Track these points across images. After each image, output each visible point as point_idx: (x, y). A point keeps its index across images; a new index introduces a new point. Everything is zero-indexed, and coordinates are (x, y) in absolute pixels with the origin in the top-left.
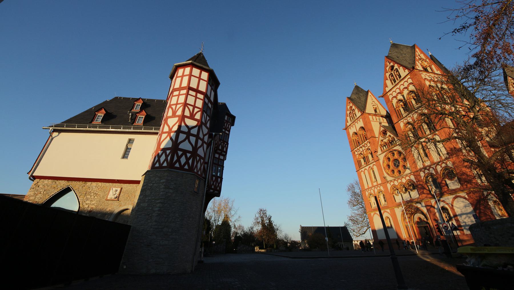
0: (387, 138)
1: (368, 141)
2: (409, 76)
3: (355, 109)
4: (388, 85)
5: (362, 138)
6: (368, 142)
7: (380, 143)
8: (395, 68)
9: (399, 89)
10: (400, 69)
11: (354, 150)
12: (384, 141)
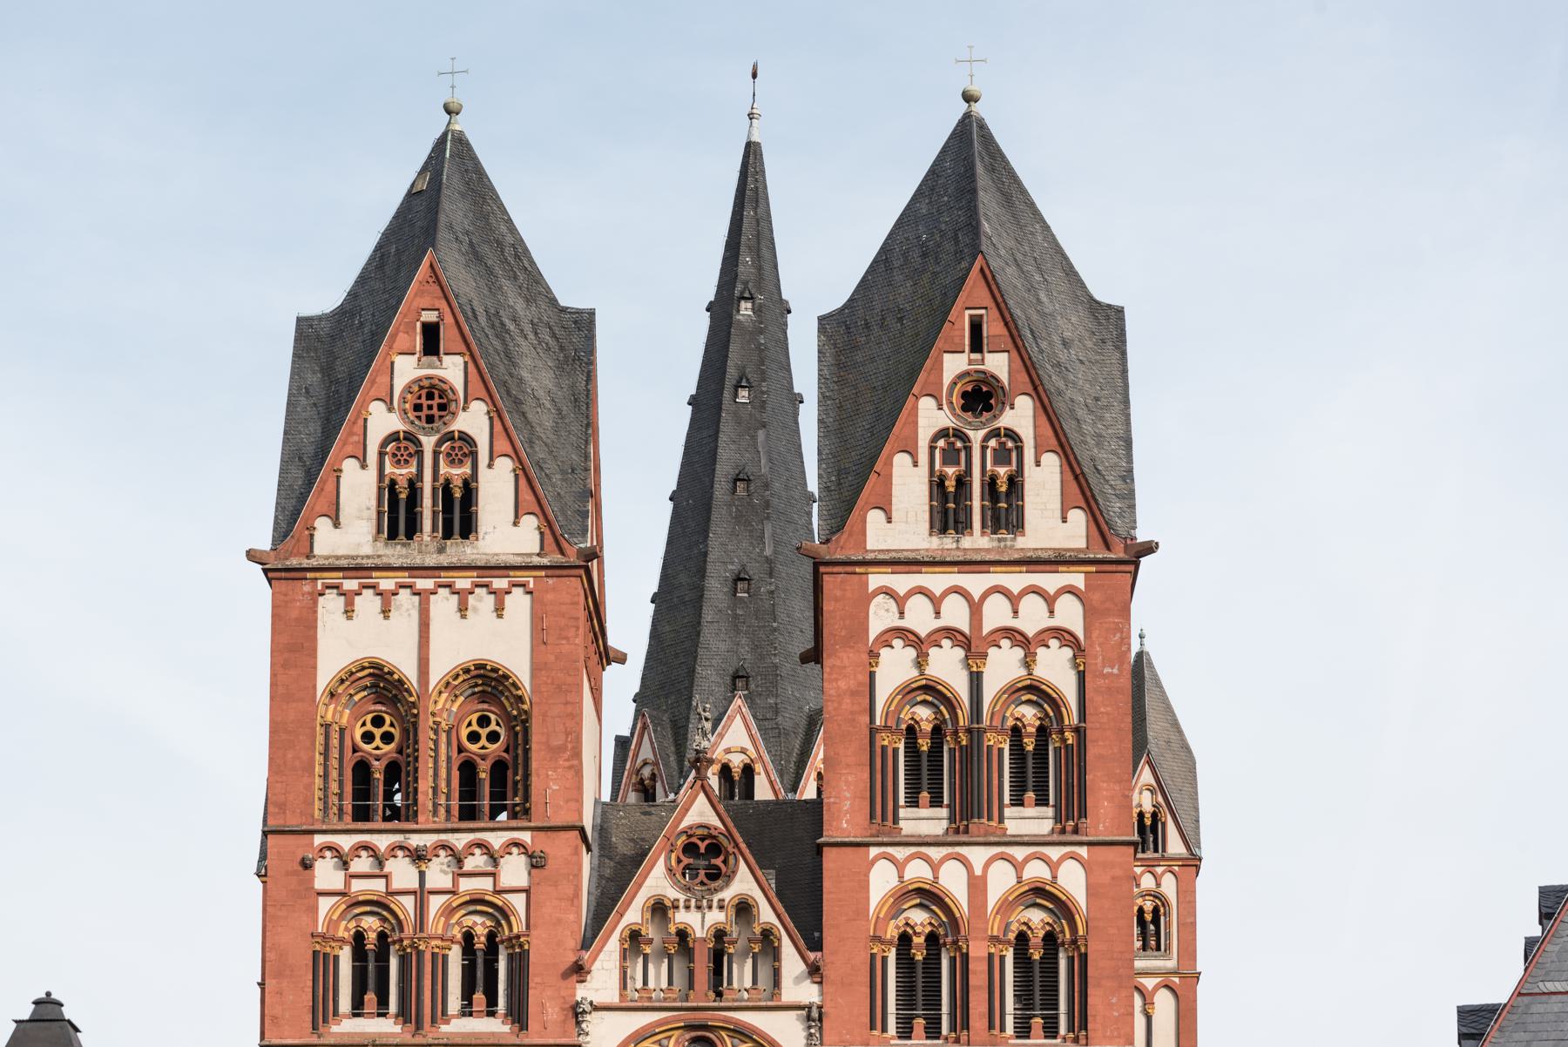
0: (721, 907)
1: (526, 837)
2: (1077, 579)
3: (490, 466)
4: (894, 500)
5: (443, 773)
6: (517, 844)
7: (633, 914)
8: (1007, 420)
9: (976, 609)
10: (1038, 464)
11: (319, 840)
12: (682, 917)
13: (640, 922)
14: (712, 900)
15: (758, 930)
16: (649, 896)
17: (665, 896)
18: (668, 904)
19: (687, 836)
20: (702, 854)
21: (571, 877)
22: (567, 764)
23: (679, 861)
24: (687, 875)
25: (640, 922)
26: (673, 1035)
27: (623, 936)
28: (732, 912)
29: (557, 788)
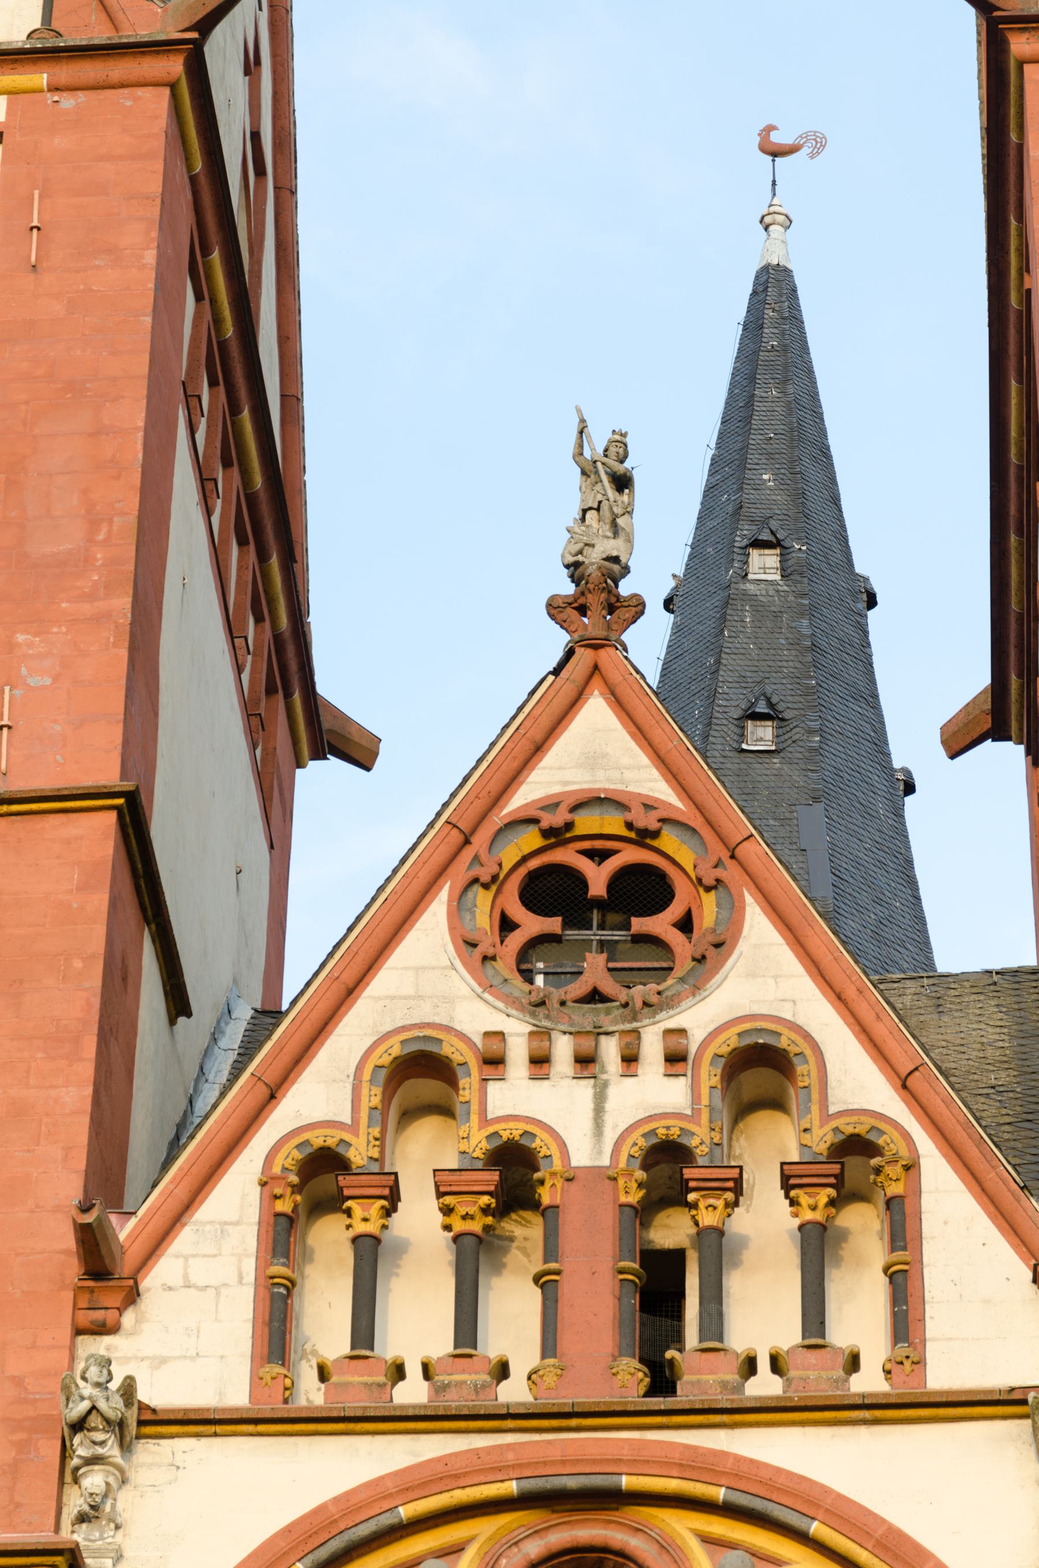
0: (675, 1059)
13: (346, 1118)
14: (636, 1032)
15: (821, 1140)
16: (388, 1027)
17: (448, 1029)
18: (451, 1049)
19: (546, 833)
20: (598, 903)
21: (78, 964)
22: (87, 609)
23: (507, 925)
24: (539, 980)
25: (346, 1118)
26: (469, 1541)
27: (277, 1170)
28: (710, 1076)
29: (48, 681)
